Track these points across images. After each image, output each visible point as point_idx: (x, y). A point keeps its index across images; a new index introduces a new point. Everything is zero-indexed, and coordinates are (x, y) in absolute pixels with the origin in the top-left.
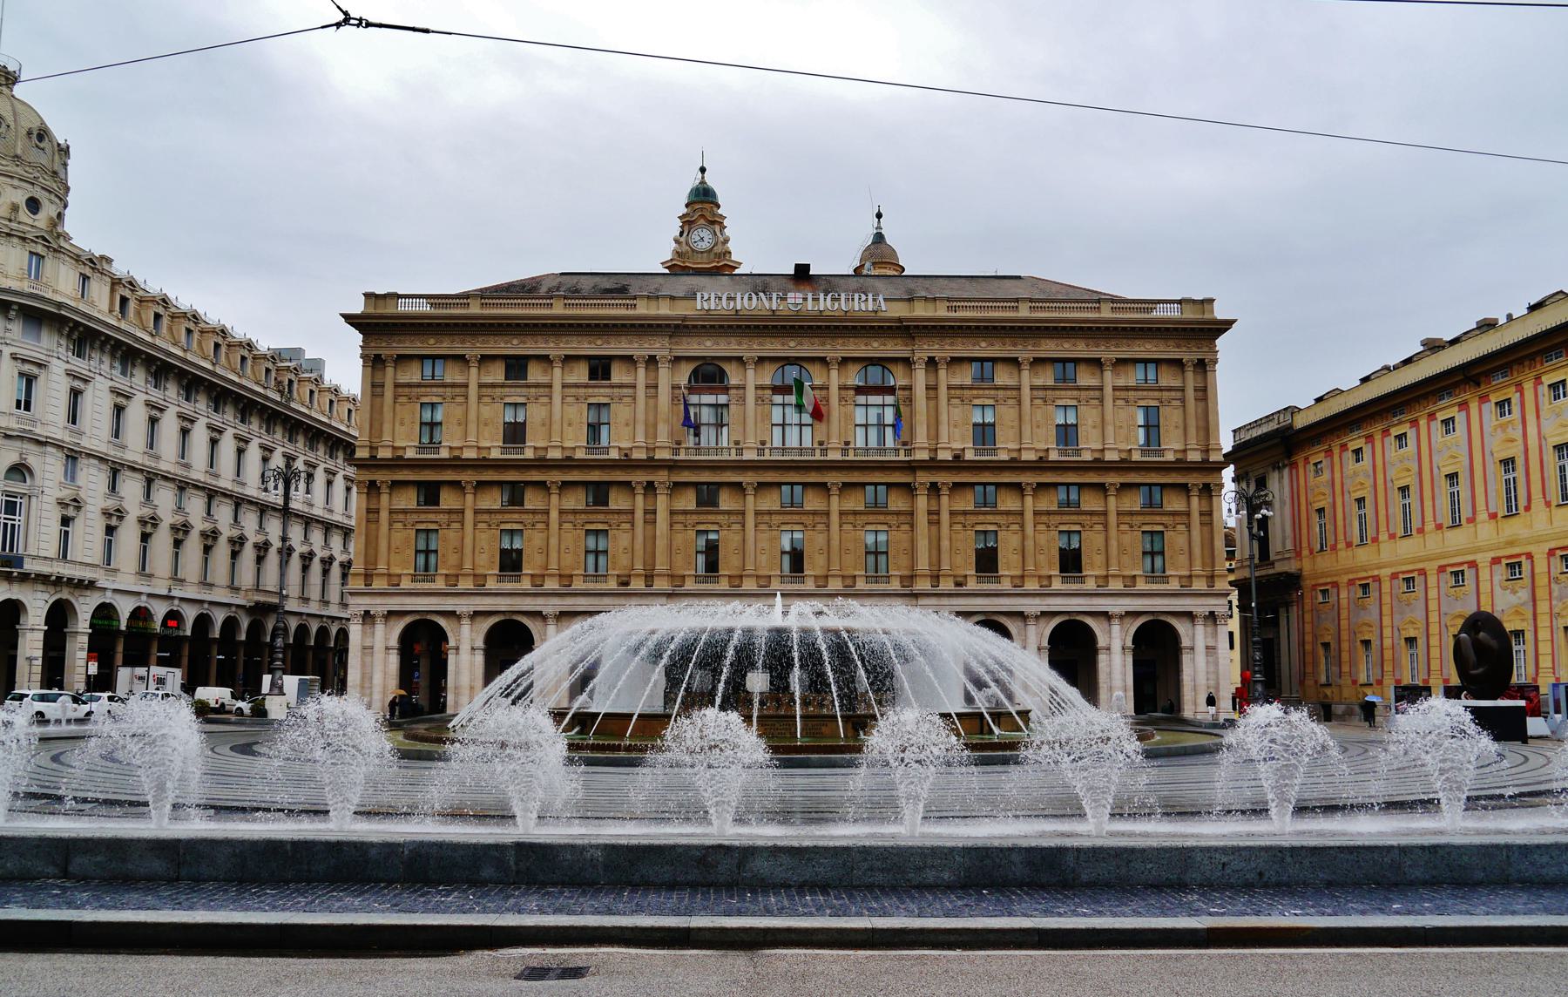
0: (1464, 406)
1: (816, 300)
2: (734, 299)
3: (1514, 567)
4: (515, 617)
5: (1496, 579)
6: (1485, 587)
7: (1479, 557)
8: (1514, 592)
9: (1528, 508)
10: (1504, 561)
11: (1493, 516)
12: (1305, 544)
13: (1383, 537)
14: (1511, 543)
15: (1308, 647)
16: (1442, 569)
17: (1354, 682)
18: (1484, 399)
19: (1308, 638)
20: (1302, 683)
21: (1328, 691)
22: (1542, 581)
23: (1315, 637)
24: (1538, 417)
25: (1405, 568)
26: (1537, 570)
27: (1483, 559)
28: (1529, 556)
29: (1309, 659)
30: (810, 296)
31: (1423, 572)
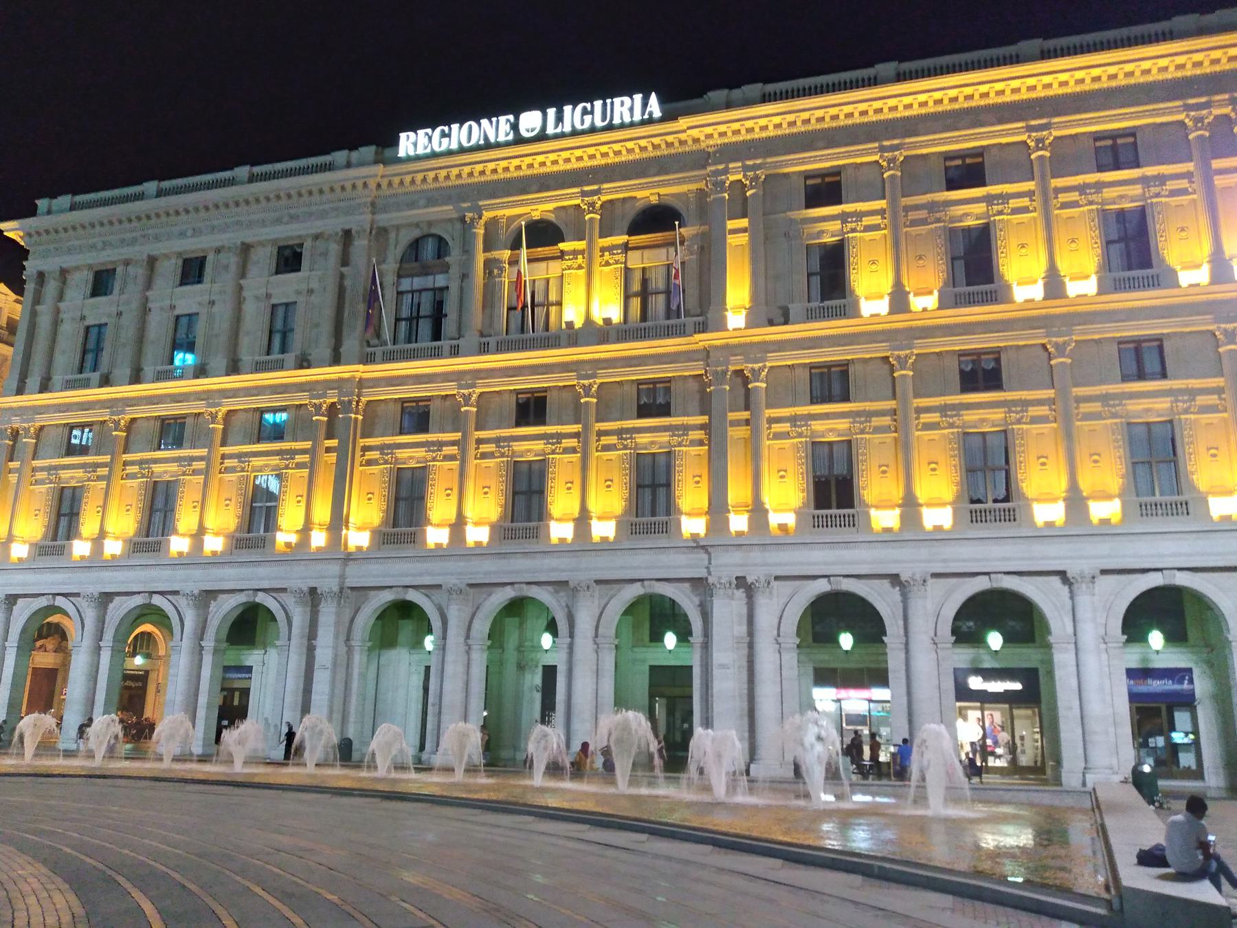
1: (559, 119)
2: (449, 136)
30: (551, 112)
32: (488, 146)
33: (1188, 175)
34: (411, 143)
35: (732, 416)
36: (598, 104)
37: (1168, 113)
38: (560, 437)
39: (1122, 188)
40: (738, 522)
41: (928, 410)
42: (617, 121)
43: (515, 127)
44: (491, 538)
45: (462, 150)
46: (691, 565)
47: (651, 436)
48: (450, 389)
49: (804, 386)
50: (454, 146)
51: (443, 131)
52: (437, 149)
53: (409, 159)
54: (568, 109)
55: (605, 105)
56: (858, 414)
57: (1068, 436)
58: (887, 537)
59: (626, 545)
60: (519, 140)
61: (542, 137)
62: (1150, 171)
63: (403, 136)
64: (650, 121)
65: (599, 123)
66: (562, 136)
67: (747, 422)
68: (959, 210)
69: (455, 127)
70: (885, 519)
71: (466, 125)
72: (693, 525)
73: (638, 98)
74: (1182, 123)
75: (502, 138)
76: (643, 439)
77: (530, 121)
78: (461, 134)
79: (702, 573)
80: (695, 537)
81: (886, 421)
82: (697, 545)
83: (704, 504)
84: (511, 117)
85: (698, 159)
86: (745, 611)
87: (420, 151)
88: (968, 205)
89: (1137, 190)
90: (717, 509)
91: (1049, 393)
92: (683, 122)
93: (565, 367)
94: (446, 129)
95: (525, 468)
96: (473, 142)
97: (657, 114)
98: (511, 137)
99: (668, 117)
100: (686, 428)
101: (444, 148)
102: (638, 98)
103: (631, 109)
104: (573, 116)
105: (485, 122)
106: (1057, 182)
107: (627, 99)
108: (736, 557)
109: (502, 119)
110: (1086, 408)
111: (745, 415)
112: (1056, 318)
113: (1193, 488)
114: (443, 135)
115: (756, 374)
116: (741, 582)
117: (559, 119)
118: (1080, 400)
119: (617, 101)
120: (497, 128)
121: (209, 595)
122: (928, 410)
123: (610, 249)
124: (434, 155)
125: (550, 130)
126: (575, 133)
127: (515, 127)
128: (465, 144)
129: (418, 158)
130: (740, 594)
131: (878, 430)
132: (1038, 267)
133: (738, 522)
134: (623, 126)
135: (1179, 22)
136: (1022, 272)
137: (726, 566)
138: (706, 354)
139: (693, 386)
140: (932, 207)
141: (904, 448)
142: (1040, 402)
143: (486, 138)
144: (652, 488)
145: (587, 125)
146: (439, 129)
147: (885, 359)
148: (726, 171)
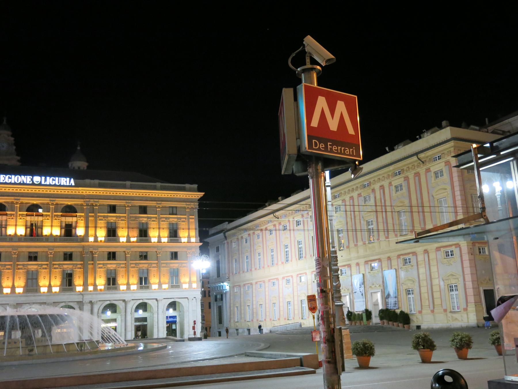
1: (45, 180)
2: (11, 178)
10: (286, 278)
12: (231, 271)
13: (266, 266)
15: (232, 308)
17: (245, 321)
19: (232, 305)
20: (230, 321)
21: (237, 324)
23: (234, 305)
29: (232, 312)
32: (24, 184)
33: (185, 218)
35: (89, 262)
36: (57, 178)
37: (183, 205)
38: (42, 265)
39: (173, 219)
40: (91, 288)
41: (133, 264)
43: (32, 180)
45: (15, 184)
46: (78, 298)
47: (68, 266)
48: (10, 250)
49: (106, 256)
50: (13, 182)
52: (7, 182)
56: (118, 264)
58: (123, 292)
60: (33, 184)
61: (40, 184)
64: (71, 186)
65: (57, 184)
67: (92, 264)
68: (141, 219)
69: (13, 176)
70: (123, 288)
71: (17, 176)
72: (79, 289)
73: (68, 179)
75: (28, 182)
77: (37, 179)
79: (81, 300)
80: (79, 291)
81: (124, 265)
82: (80, 293)
83: (82, 283)
84: (31, 177)
85: (82, 197)
86: (90, 308)
88: (143, 218)
89: (176, 220)
90: (85, 285)
91: (157, 262)
92: (80, 188)
93: (44, 247)
94: (10, 176)
95: (31, 272)
96: (19, 182)
97: (73, 184)
98: (31, 183)
99: (76, 186)
101: (9, 182)
102: (68, 179)
104: (50, 180)
105: (23, 177)
107: (65, 179)
108: (90, 296)
109: (28, 177)
110: (163, 265)
111: (92, 262)
113: (181, 283)
114: (9, 178)
116: (91, 302)
117: (45, 180)
118: (162, 263)
119: (62, 179)
120: (27, 179)
122: (133, 264)
123: (57, 216)
124: (6, 183)
126: (50, 185)
127: (32, 180)
128: (16, 182)
130: (89, 305)
131: (122, 267)
132: (157, 234)
133: (91, 288)
134: (64, 186)
136: (153, 234)
137: (87, 298)
138: (83, 247)
139: (79, 253)
140: (136, 217)
141: (128, 272)
142: (154, 263)
143: (23, 181)
144: (68, 281)
145: (53, 184)
146: (8, 176)
147: (125, 252)
148: (89, 201)
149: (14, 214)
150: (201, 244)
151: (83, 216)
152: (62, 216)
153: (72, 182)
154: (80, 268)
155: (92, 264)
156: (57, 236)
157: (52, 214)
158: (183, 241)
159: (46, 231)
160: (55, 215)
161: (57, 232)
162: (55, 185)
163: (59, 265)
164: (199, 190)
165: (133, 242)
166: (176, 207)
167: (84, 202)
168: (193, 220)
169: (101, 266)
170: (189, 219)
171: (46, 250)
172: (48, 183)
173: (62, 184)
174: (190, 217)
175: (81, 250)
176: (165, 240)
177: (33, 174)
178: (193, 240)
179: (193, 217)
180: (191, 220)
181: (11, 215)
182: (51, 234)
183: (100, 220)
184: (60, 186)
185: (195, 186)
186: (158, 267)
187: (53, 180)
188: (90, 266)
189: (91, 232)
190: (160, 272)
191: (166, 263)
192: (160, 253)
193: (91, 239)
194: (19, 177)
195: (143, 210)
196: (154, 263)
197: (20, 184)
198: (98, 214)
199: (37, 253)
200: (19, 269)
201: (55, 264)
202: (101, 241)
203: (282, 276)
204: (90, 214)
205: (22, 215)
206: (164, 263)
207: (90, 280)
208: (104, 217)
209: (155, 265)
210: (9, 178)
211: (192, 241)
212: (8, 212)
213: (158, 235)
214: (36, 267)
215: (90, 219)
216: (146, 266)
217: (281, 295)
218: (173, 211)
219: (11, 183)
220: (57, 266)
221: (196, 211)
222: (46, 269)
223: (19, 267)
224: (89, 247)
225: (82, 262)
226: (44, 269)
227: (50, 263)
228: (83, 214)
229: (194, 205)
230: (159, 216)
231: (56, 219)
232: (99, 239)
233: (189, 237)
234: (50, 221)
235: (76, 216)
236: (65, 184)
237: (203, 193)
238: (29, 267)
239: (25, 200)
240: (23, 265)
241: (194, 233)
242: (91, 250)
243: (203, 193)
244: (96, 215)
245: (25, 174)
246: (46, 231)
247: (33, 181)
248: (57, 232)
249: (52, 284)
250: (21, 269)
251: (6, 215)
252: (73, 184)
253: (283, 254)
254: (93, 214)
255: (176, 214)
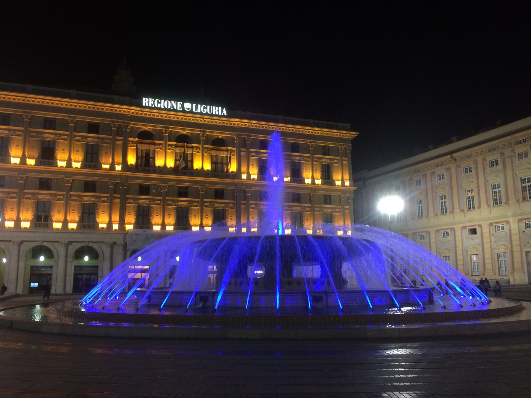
0: (449, 169)
1: (197, 108)
2: (160, 103)
3: (474, 231)
4: (45, 244)
5: (464, 235)
6: (458, 238)
7: (455, 227)
8: (472, 239)
9: (479, 207)
11: (463, 211)
14: (471, 221)
16: (437, 231)
18: (458, 166)
22: (486, 235)
24: (484, 173)
25: (419, 231)
26: (484, 231)
27: (458, 227)
28: (480, 226)
30: (194, 105)
31: (453, 229)
32: (174, 110)
34: (146, 101)
35: (243, 202)
36: (208, 107)
42: (214, 113)
43: (183, 106)
44: (30, 226)
45: (165, 109)
48: (159, 183)
50: (162, 107)
51: (158, 101)
53: (146, 107)
54: (199, 106)
55: (210, 108)
57: (314, 215)
59: (33, 230)
60: (184, 111)
61: (191, 112)
62: (332, 157)
63: (144, 99)
64: (223, 116)
65: (209, 112)
66: (197, 113)
67: (245, 204)
68: (294, 158)
69: (163, 101)
71: (166, 102)
73: (220, 108)
74: (338, 147)
75: (178, 109)
76: (217, 205)
78: (164, 104)
87: (150, 105)
88: (296, 156)
91: (310, 205)
92: (233, 119)
96: (169, 107)
97: (226, 114)
99: (229, 116)
100: (229, 203)
102: (220, 108)
103: (218, 111)
104: (201, 108)
105: (173, 102)
106: (314, 156)
109: (179, 103)
111: (244, 202)
112: (313, 187)
115: (248, 192)
119: (214, 107)
120: (178, 105)
121: (70, 243)
123: (208, 148)
124: (155, 108)
125: (194, 110)
126: (201, 113)
127: (183, 106)
129: (149, 108)
134: (216, 115)
135: (341, 124)
138: (236, 184)
142: (308, 207)
145: (205, 112)
146: (157, 100)
148: (241, 135)
149: (162, 144)
150: (355, 188)
151: (234, 151)
152: (212, 149)
153: (225, 112)
154: (232, 208)
155: (245, 204)
156: (208, 170)
157: (203, 146)
158: (336, 184)
159: (197, 164)
160: (206, 148)
161: (208, 166)
162: (207, 114)
163: (210, 202)
164: (352, 130)
165: (287, 182)
166: (329, 147)
167: (236, 135)
168: (346, 162)
169: (254, 206)
170: (343, 160)
171: (197, 185)
172: (199, 111)
173: (214, 113)
174: (344, 158)
175: (233, 188)
176: (319, 182)
177: (184, 101)
178: (347, 183)
179: (346, 159)
180: (344, 162)
181: (160, 144)
182: (202, 168)
183: (252, 156)
184: (212, 115)
185: (348, 125)
186: (312, 210)
187: (204, 108)
188: (243, 206)
189: (244, 169)
190: (314, 215)
191: (320, 207)
192: (313, 195)
193: (244, 176)
194: (169, 102)
195: (295, 148)
196: (308, 207)
197: (170, 110)
198: (251, 150)
199: (187, 188)
200: (169, 205)
201: (206, 202)
202: (254, 179)
203: (461, 225)
204: (242, 149)
205: (171, 145)
206: (317, 207)
207: (244, 221)
208: (256, 152)
209: (308, 209)
210: (158, 102)
211: (346, 185)
212: (156, 142)
213: (311, 177)
214: (186, 204)
215: (243, 154)
216: (299, 209)
217: (459, 248)
218: (326, 151)
219: (160, 109)
220: (208, 204)
221: (349, 152)
222: (196, 206)
223: (169, 202)
224: (242, 184)
225: (234, 201)
226: (194, 206)
227: (202, 200)
228: (234, 149)
229: (347, 146)
230: (312, 156)
231: (206, 153)
232: (252, 177)
233: (343, 181)
234: (200, 153)
235: (227, 150)
236: (217, 114)
237: (357, 133)
238: (180, 203)
239: (174, 129)
240: (173, 201)
241: (346, 177)
242: (244, 188)
243: (357, 133)
244: (248, 150)
245: (176, 99)
246: (197, 164)
247: (183, 108)
248: (208, 166)
249: (204, 223)
250: (171, 205)
251: (155, 144)
252: (226, 114)
253: (439, 206)
254: (245, 150)
255: (328, 155)
